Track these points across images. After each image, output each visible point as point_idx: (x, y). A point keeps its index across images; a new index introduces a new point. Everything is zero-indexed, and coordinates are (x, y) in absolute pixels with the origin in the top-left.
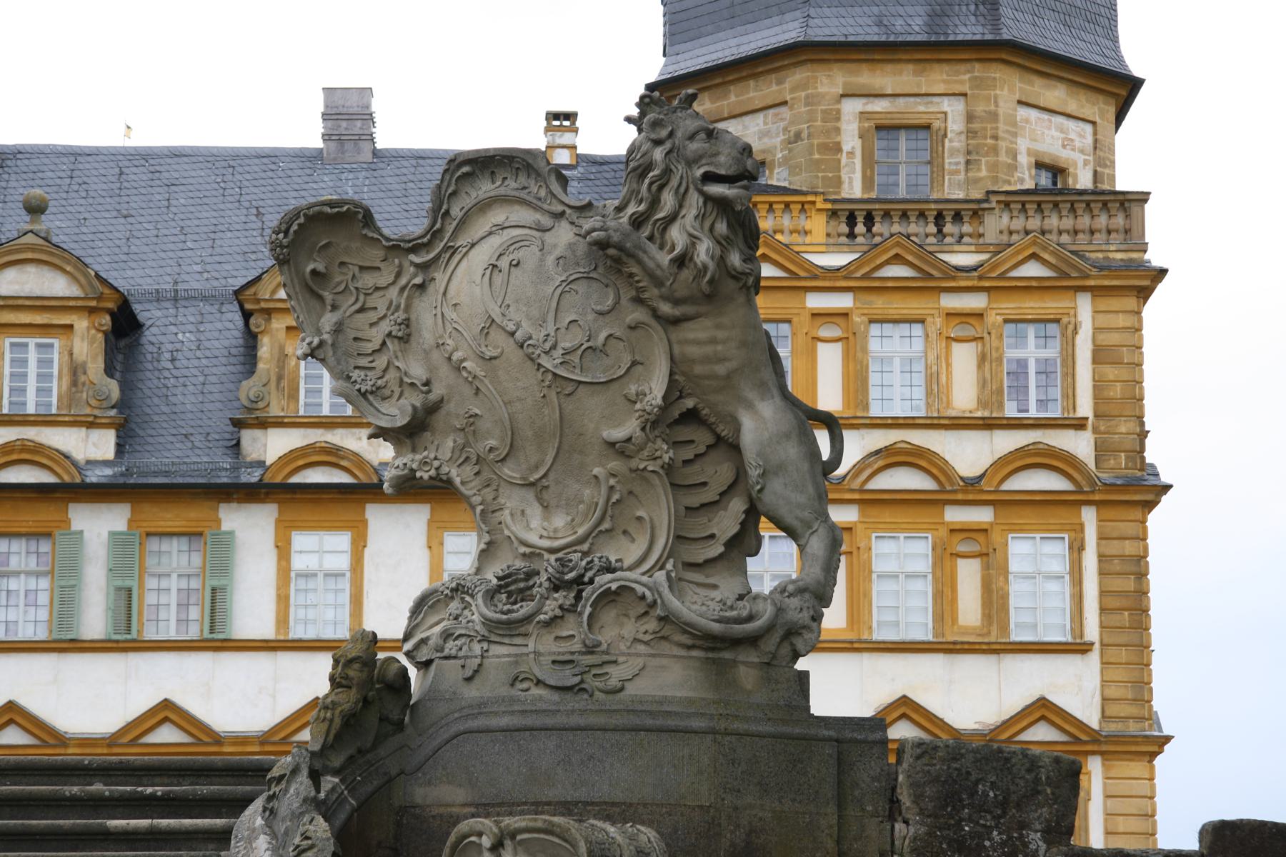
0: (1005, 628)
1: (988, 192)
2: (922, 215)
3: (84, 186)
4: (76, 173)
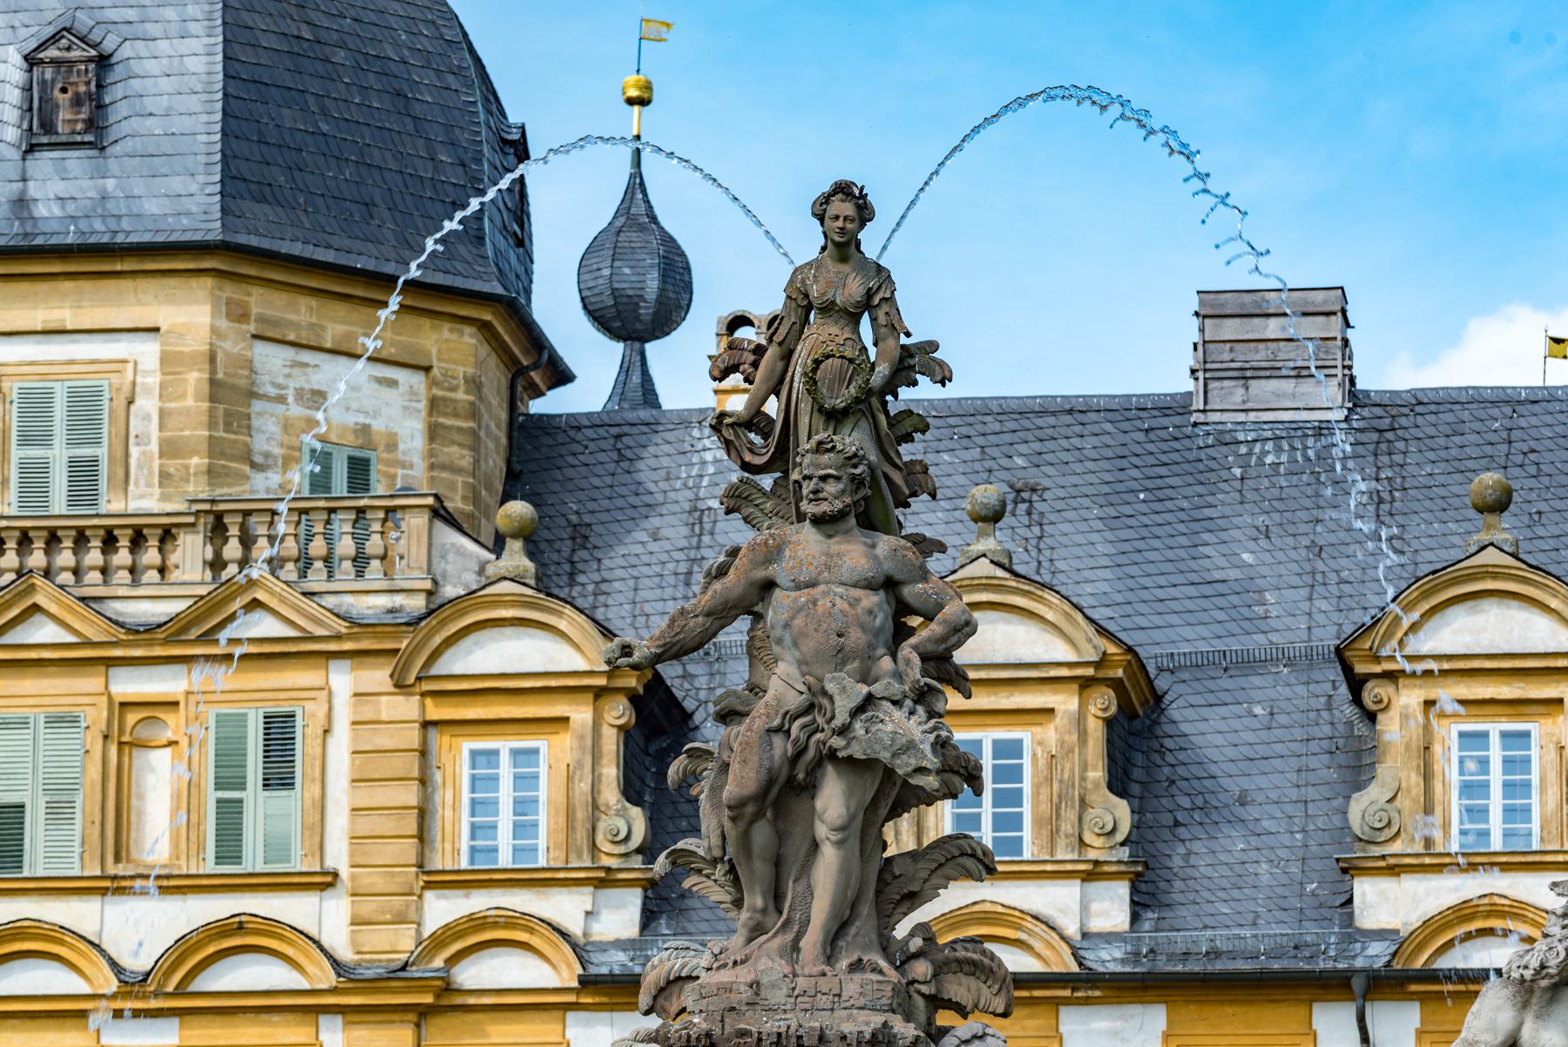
3: (1532, 456)
4: (1516, 435)
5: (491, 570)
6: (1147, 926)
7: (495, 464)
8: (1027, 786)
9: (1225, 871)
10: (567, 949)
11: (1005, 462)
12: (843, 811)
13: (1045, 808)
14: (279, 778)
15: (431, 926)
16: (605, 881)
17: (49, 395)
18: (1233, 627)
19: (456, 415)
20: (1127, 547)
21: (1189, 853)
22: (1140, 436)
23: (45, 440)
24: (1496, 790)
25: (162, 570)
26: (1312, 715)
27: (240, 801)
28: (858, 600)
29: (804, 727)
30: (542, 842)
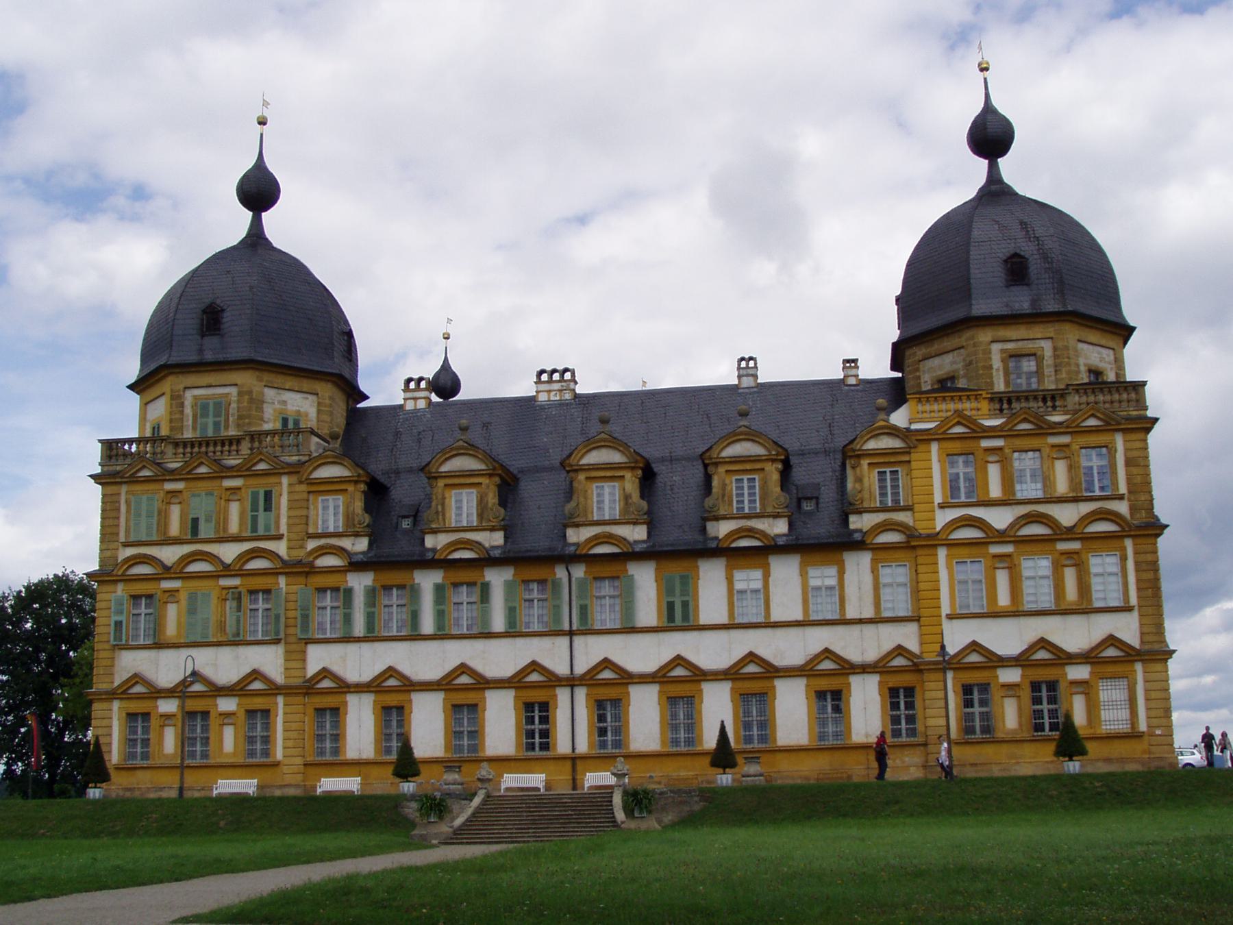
0: (1090, 601)
1: (1068, 385)
2: (1035, 398)
14: (268, 508)
16: (357, 535)
17: (208, 404)
19: (325, 406)
25: (237, 451)
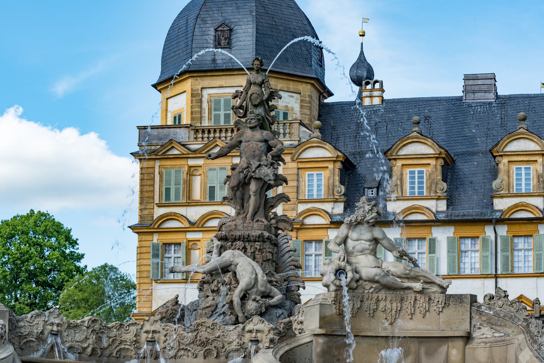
4: (531, 104)
5: (312, 136)
6: (450, 209)
7: (316, 113)
8: (425, 180)
9: (467, 198)
10: (328, 216)
11: (423, 111)
12: (255, 189)
13: (429, 185)
15: (299, 211)
16: (336, 201)
17: (220, 100)
18: (470, 146)
20: (448, 129)
21: (460, 194)
22: (452, 105)
23: (219, 110)
24: (523, 180)
26: (486, 164)
27: (170, 188)
28: (258, 144)
29: (247, 171)
30: (323, 194)
